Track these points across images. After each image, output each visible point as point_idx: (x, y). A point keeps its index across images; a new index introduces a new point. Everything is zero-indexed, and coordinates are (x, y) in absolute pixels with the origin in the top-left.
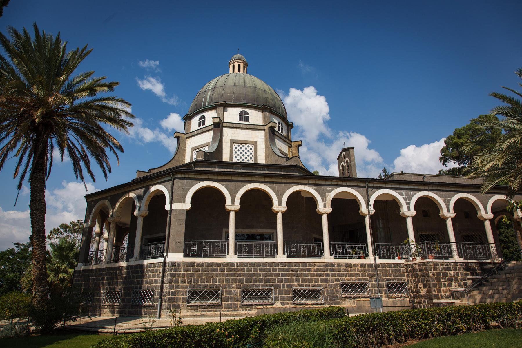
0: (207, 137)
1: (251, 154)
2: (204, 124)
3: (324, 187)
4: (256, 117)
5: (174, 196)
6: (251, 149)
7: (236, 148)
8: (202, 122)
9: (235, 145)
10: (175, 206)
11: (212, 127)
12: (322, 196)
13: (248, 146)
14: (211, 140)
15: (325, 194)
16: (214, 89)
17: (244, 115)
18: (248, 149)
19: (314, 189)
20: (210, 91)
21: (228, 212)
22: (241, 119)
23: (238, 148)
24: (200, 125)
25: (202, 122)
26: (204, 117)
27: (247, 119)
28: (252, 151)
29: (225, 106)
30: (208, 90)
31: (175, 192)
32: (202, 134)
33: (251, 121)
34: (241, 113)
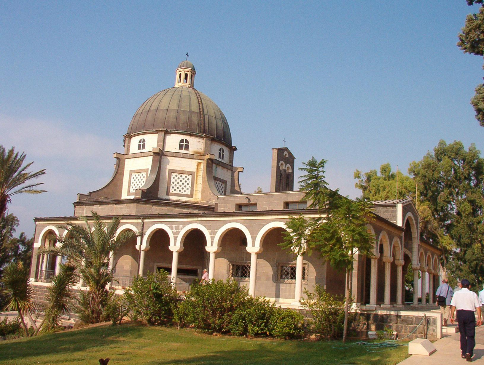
0: (147, 163)
1: (188, 184)
4: (197, 144)
6: (188, 179)
7: (174, 178)
8: (142, 145)
9: (173, 175)
11: (152, 154)
13: (186, 177)
14: (149, 167)
17: (184, 144)
18: (186, 179)
22: (181, 147)
23: (176, 178)
24: (139, 149)
25: (142, 145)
26: (144, 141)
27: (187, 147)
28: (189, 182)
29: (167, 133)
33: (191, 151)
34: (182, 141)
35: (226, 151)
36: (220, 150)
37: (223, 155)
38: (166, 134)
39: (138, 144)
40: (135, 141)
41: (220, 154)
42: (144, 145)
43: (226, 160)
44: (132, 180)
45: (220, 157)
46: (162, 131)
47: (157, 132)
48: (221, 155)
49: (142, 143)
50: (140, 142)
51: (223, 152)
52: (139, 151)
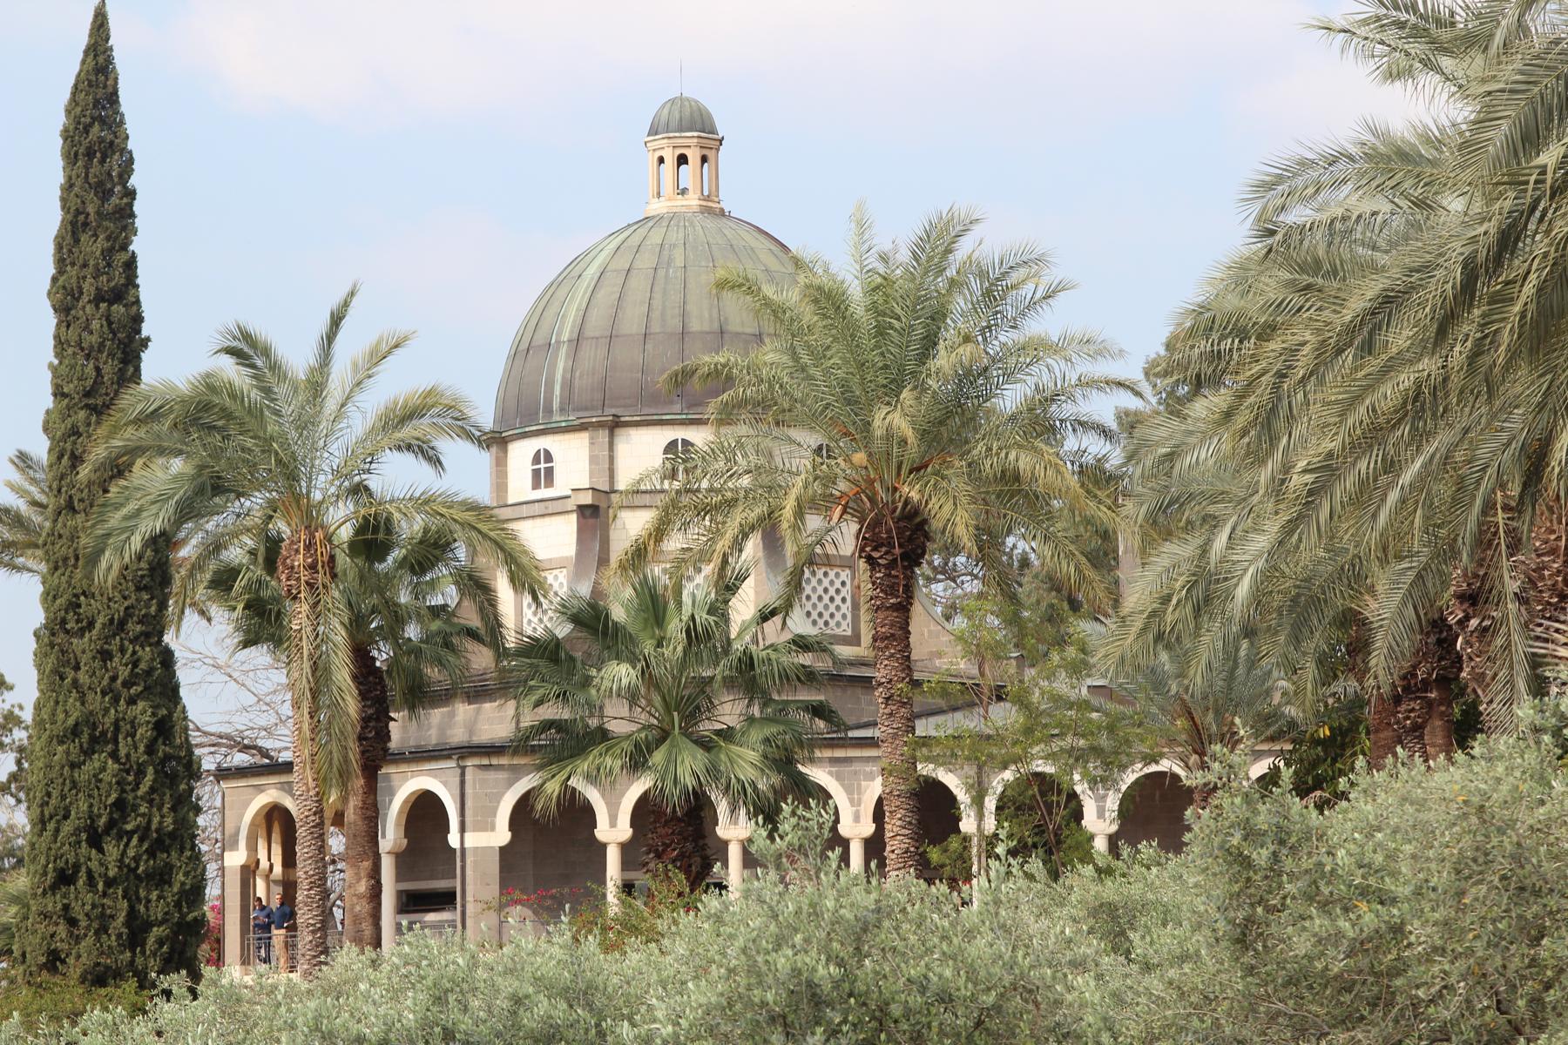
2: (550, 482)
3: (856, 767)
5: (468, 812)
8: (543, 474)
10: (472, 840)
12: (849, 790)
15: (859, 786)
16: (577, 341)
19: (830, 773)
20: (563, 350)
21: (604, 846)
24: (536, 486)
25: (543, 474)
29: (615, 426)
30: (558, 342)
31: (469, 804)
32: (547, 520)
34: (671, 447)
38: (619, 431)
39: (529, 468)
40: (521, 454)
42: (550, 471)
46: (600, 425)
47: (582, 428)
49: (542, 466)
50: (536, 460)
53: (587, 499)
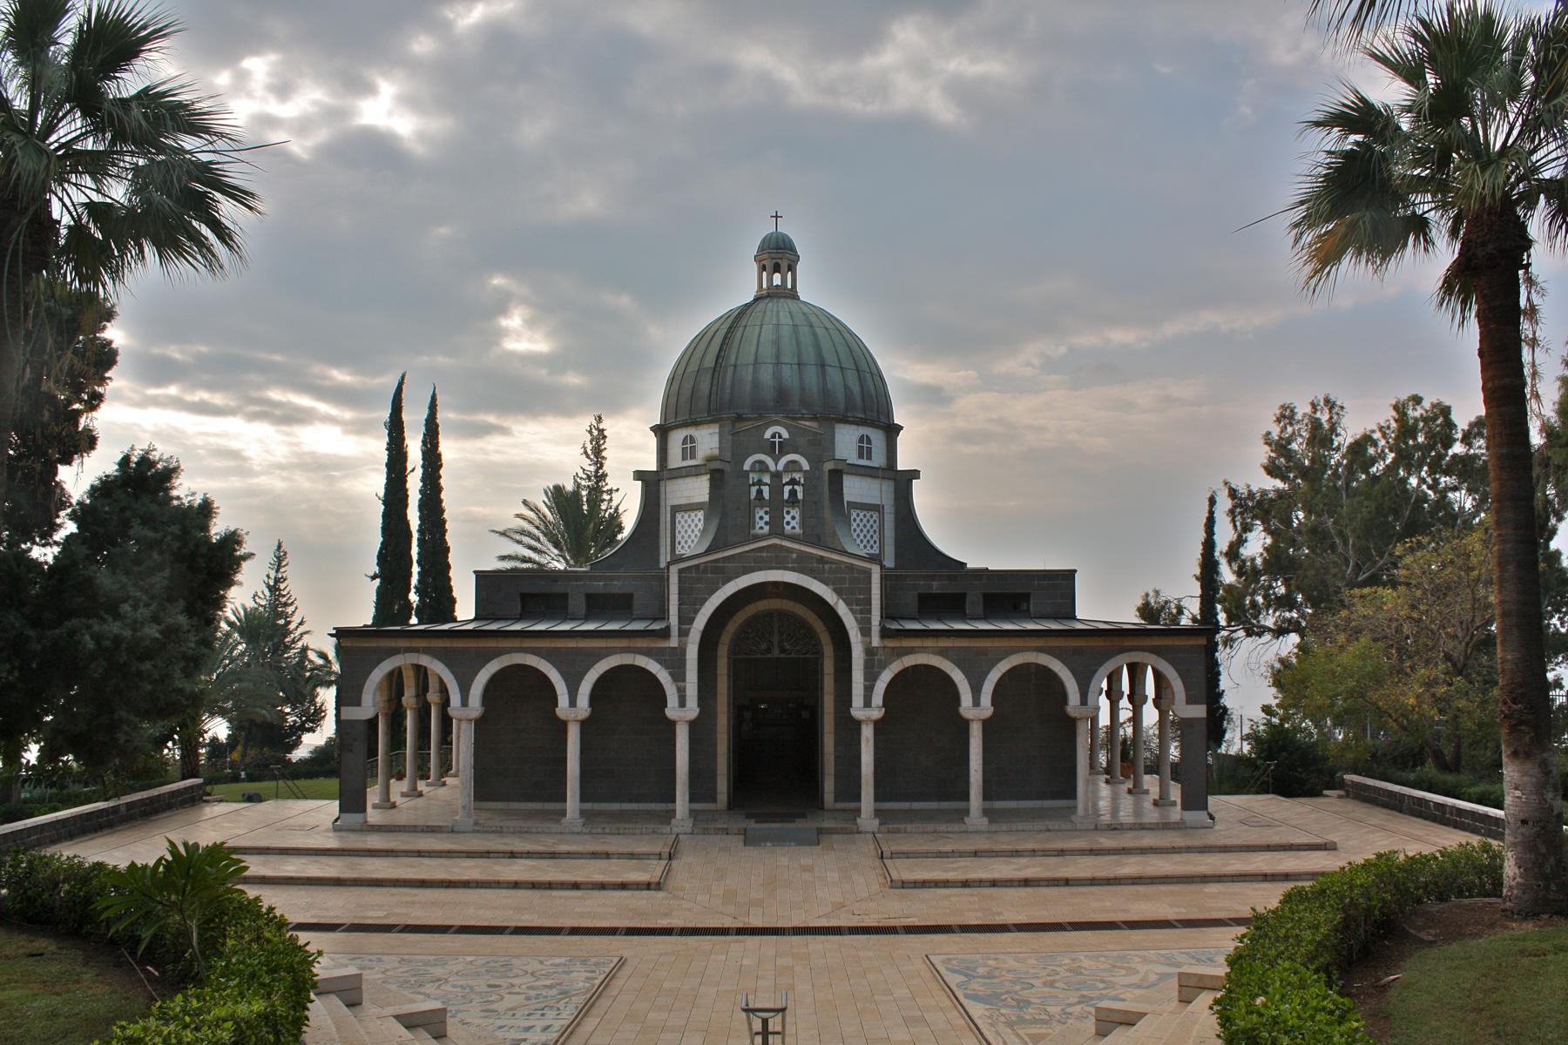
2: (693, 456)
8: (689, 450)
25: (689, 450)
26: (692, 440)
35: (877, 438)
36: (861, 440)
37: (869, 450)
41: (861, 448)
42: (693, 449)
43: (878, 460)
44: (678, 527)
45: (861, 456)
48: (864, 450)
51: (869, 441)
52: (685, 463)
53: (716, 465)
